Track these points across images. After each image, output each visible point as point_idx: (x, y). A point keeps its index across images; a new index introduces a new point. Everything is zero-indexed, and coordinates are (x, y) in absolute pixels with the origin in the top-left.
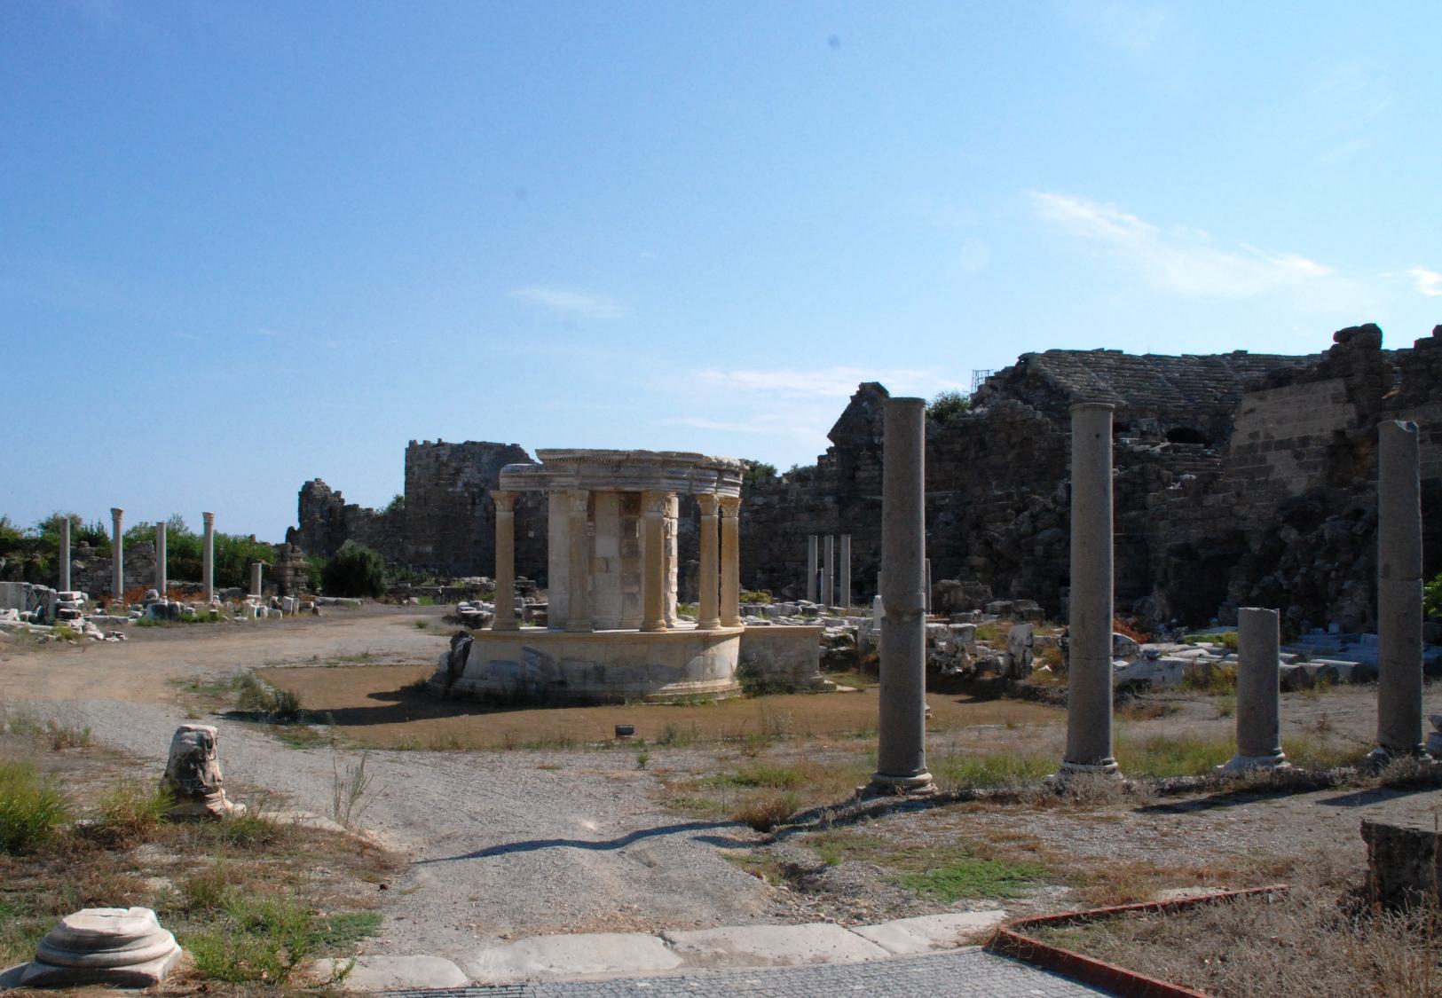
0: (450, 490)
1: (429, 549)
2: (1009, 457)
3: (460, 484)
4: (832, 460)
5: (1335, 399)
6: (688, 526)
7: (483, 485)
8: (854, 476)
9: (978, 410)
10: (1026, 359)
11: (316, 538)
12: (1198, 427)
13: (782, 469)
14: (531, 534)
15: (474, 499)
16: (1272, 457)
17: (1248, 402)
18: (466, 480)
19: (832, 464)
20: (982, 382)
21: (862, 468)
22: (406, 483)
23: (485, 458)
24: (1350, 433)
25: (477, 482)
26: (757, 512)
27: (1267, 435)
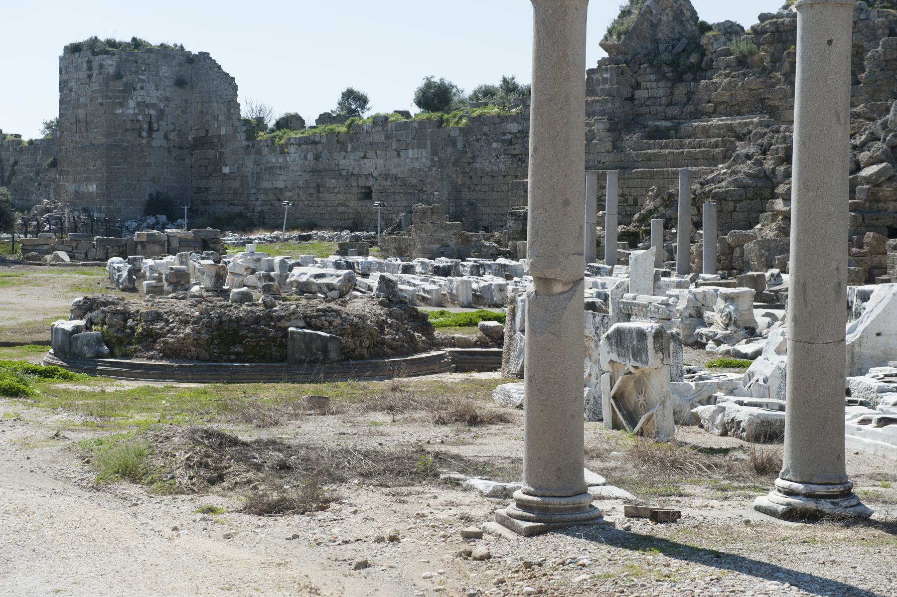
0: (119, 111)
1: (93, 188)
3: (132, 104)
4: (605, 76)
6: (424, 160)
7: (162, 106)
8: (633, 95)
14: (226, 170)
15: (150, 123)
18: (139, 99)
19: (605, 80)
21: (643, 85)
22: (61, 102)
25: (154, 101)
26: (510, 143)
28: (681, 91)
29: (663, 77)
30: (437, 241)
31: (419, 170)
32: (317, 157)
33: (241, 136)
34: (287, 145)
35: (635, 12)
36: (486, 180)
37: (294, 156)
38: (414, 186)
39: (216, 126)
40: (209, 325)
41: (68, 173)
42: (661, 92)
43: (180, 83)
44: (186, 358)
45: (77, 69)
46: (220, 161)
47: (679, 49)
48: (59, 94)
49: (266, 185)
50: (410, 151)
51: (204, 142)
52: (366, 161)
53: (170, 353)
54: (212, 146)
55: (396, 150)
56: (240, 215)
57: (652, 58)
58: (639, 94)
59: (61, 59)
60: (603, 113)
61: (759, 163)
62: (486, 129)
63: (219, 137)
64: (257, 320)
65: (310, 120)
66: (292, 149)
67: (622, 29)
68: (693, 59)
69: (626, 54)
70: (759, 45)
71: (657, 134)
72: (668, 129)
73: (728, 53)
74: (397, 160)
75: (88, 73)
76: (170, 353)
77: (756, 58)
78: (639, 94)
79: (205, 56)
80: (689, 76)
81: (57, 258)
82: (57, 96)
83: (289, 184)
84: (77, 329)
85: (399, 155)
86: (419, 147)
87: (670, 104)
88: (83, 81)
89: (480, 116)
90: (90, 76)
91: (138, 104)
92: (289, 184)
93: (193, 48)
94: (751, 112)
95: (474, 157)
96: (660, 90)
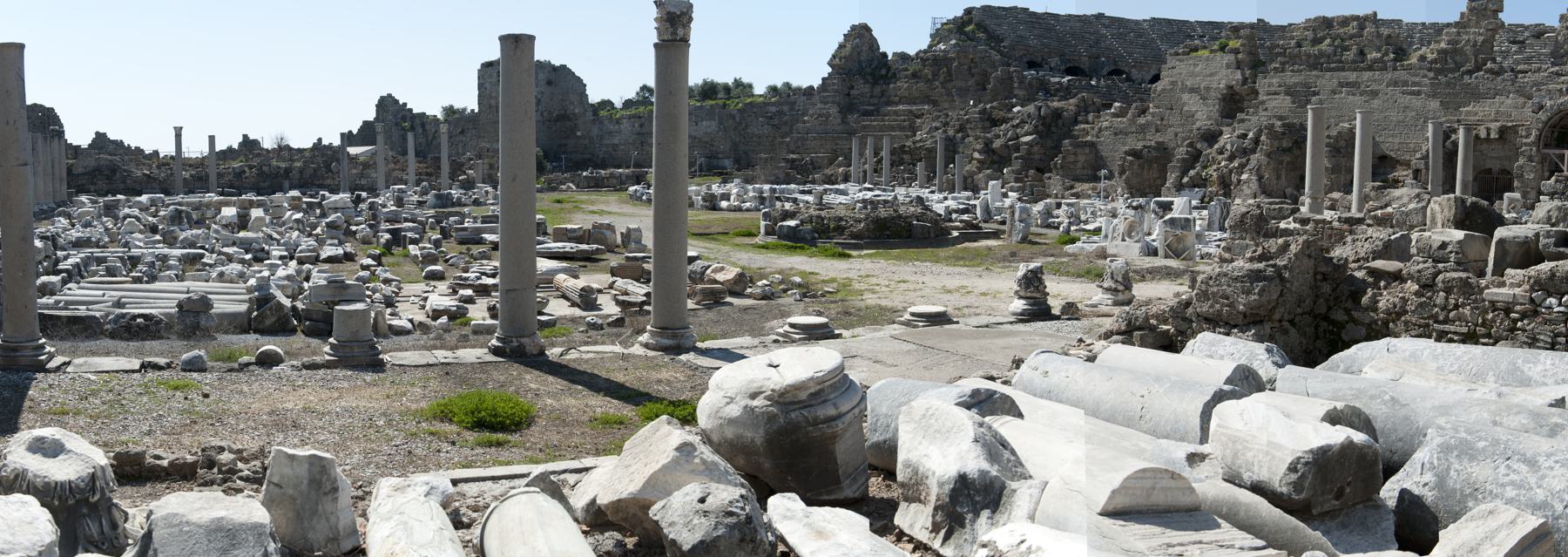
2: (970, 83)
5: (1228, 66)
9: (942, 47)
10: (969, 11)
11: (394, 139)
12: (1082, 66)
13: (804, 87)
14: (579, 134)
16: (1186, 97)
17: (1171, 61)
19: (834, 84)
20: (939, 26)
22: (479, 96)
23: (541, 76)
24: (1237, 88)
26: (771, 118)
27: (1183, 84)
28: (878, 90)
29: (867, 82)
30: (774, 175)
32: (641, 126)
33: (589, 115)
34: (620, 118)
35: (849, 46)
36: (754, 139)
37: (625, 124)
38: (707, 143)
40: (872, 221)
41: (484, 137)
42: (867, 90)
43: (549, 83)
44: (862, 239)
45: (491, 76)
46: (575, 128)
47: (873, 66)
49: (605, 142)
50: (704, 123)
51: (563, 117)
53: (854, 236)
54: (570, 120)
56: (589, 160)
57: (861, 72)
58: (852, 92)
60: (833, 102)
61: (945, 132)
62: (755, 110)
63: (574, 115)
64: (893, 218)
65: (618, 104)
66: (624, 121)
67: (843, 55)
68: (883, 72)
69: (843, 69)
70: (925, 66)
71: (866, 113)
72: (872, 111)
73: (907, 70)
76: (854, 236)
77: (923, 73)
78: (852, 92)
79: (564, 67)
80: (882, 82)
81: (569, 187)
83: (623, 142)
84: (797, 226)
86: (710, 119)
87: (872, 97)
89: (751, 103)
92: (623, 142)
93: (557, 62)
94: (923, 103)
95: (747, 126)
96: (866, 89)
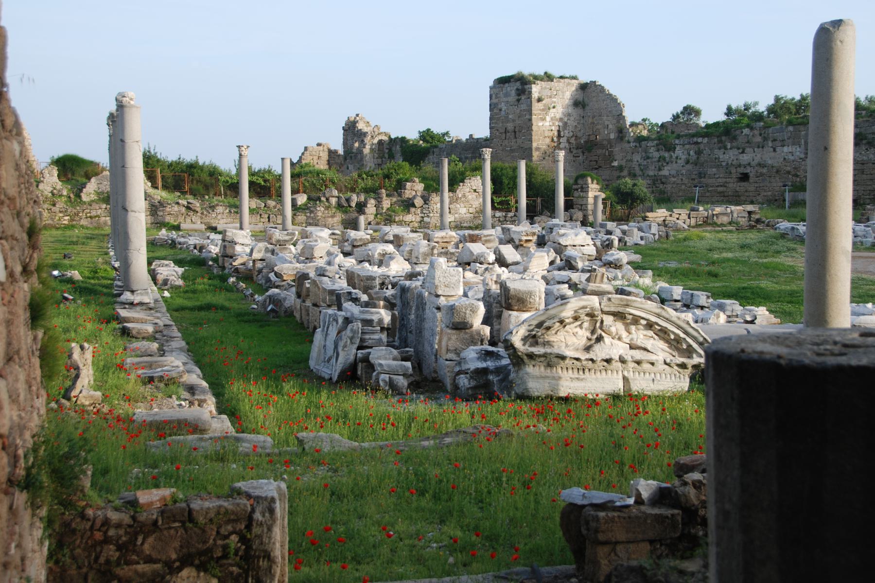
3: (548, 118)
6: (798, 153)
14: (615, 164)
18: (552, 115)
22: (491, 119)
31: (793, 161)
38: (789, 173)
39: (606, 132)
45: (507, 95)
48: (489, 113)
52: (745, 155)
55: (772, 147)
59: (491, 88)
74: (773, 154)
75: (517, 97)
82: (488, 114)
85: (775, 150)
86: (793, 144)
88: (512, 104)
90: (518, 100)
91: (552, 119)
